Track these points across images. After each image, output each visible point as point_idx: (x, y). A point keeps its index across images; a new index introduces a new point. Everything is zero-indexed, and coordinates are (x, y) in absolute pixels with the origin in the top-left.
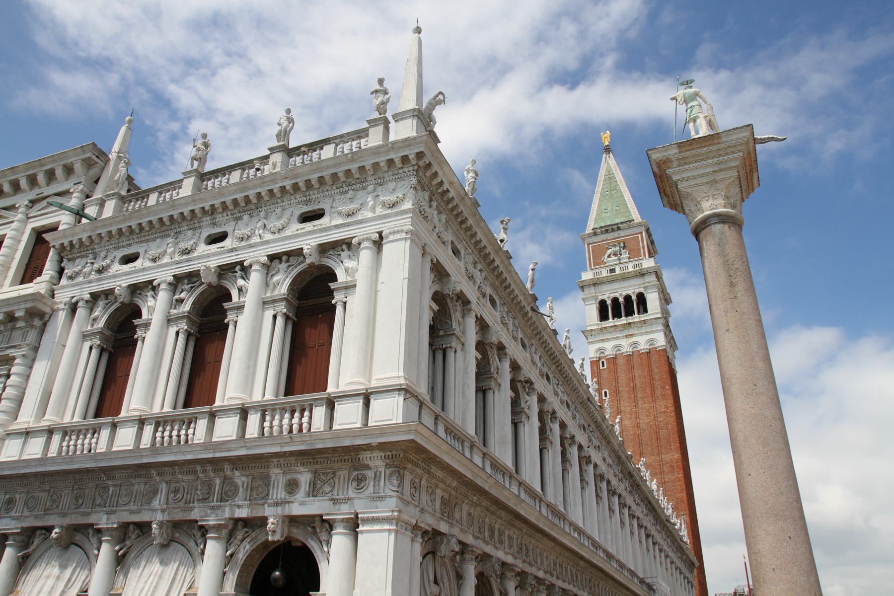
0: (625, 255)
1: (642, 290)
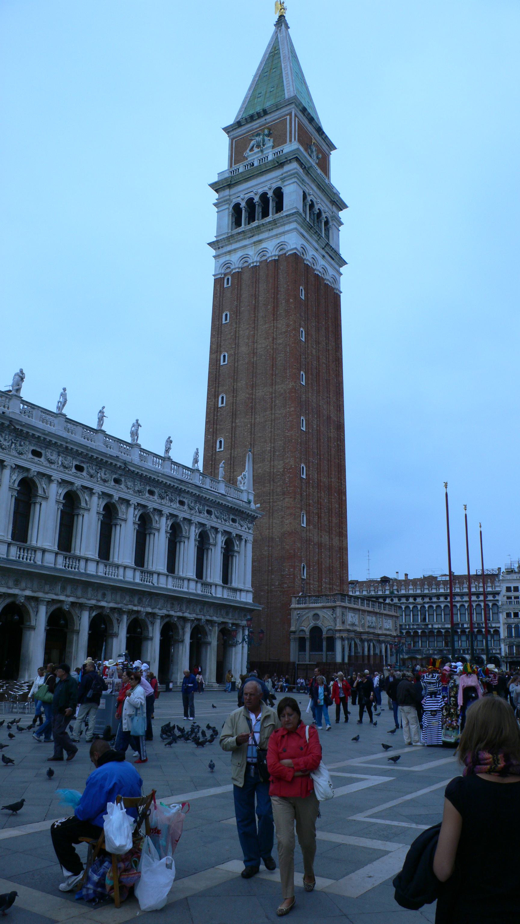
0: (269, 143)
1: (279, 184)
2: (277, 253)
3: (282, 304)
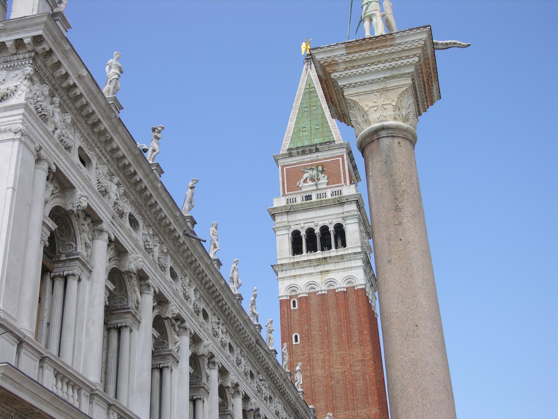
0: (324, 180)
1: (340, 221)
2: (345, 286)
3: (354, 333)
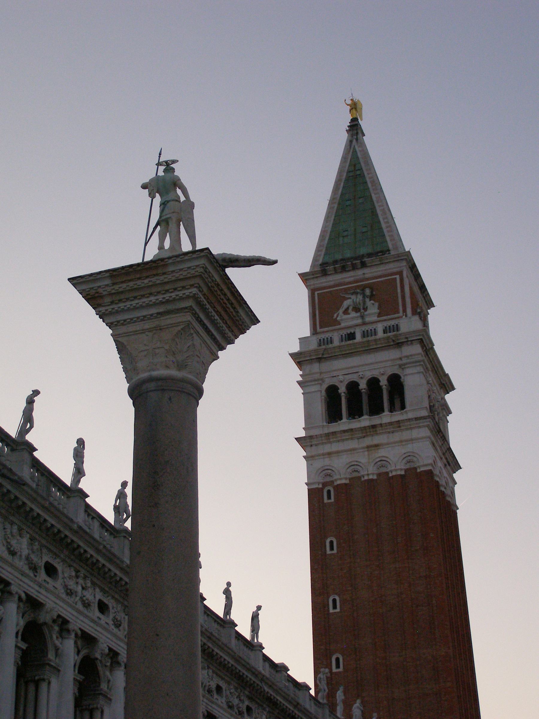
0: (373, 309)
1: (396, 370)
2: (403, 467)
